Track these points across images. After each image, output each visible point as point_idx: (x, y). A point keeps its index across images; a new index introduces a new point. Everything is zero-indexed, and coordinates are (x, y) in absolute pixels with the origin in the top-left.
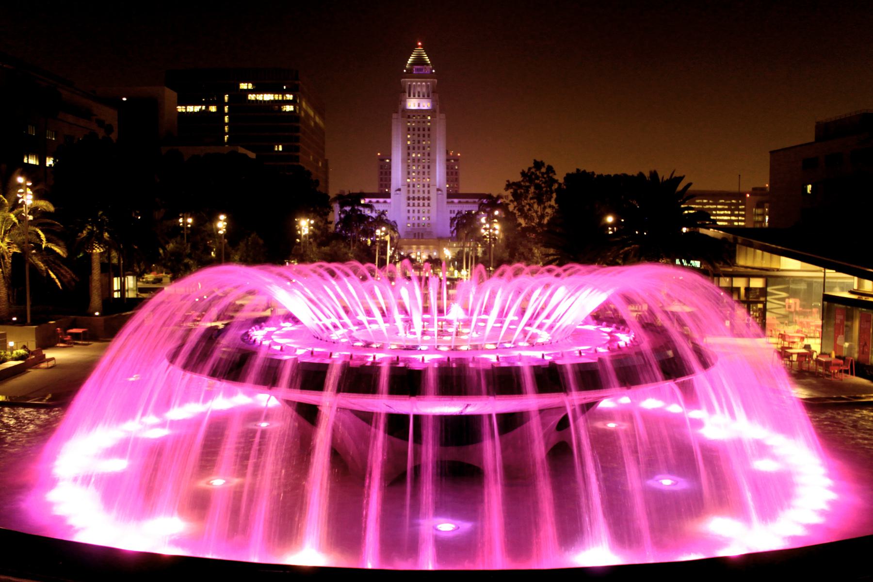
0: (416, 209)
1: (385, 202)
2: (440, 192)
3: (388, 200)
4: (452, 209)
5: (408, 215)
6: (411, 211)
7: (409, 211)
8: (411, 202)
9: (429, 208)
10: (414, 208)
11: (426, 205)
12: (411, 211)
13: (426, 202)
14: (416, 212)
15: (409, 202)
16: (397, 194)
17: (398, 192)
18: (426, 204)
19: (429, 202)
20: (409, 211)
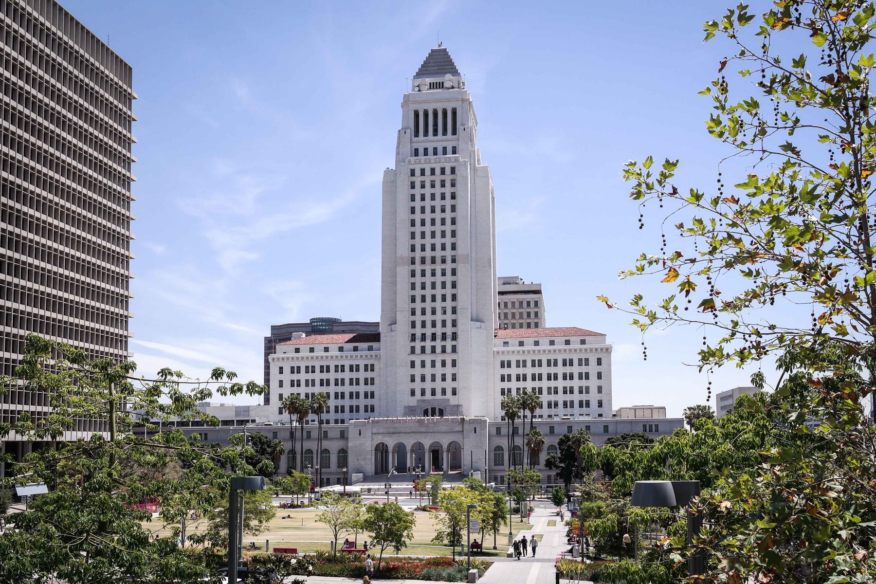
0: (428, 359)
1: (370, 349)
2: (478, 324)
3: (375, 345)
4: (506, 358)
5: (412, 371)
6: (418, 364)
7: (413, 365)
8: (418, 344)
9: (454, 356)
10: (423, 357)
11: (449, 349)
12: (418, 364)
13: (449, 344)
14: (428, 364)
15: (413, 344)
16: (391, 331)
17: (393, 326)
18: (449, 349)
19: (454, 343)
20: (413, 365)
